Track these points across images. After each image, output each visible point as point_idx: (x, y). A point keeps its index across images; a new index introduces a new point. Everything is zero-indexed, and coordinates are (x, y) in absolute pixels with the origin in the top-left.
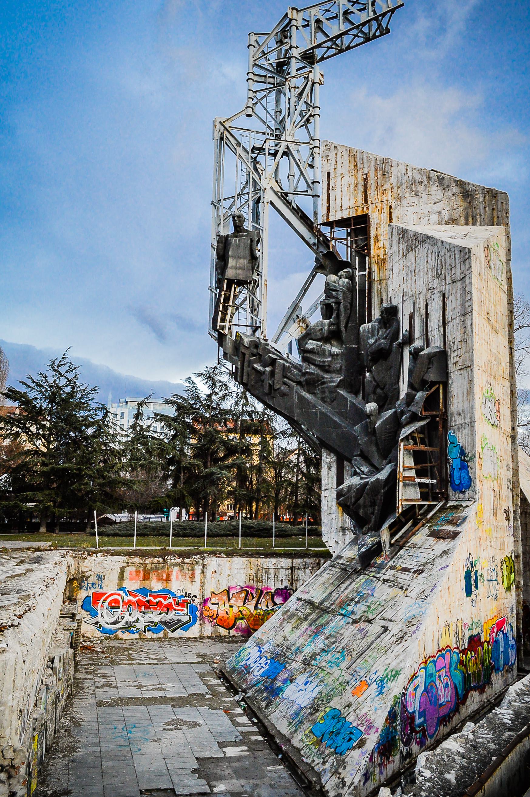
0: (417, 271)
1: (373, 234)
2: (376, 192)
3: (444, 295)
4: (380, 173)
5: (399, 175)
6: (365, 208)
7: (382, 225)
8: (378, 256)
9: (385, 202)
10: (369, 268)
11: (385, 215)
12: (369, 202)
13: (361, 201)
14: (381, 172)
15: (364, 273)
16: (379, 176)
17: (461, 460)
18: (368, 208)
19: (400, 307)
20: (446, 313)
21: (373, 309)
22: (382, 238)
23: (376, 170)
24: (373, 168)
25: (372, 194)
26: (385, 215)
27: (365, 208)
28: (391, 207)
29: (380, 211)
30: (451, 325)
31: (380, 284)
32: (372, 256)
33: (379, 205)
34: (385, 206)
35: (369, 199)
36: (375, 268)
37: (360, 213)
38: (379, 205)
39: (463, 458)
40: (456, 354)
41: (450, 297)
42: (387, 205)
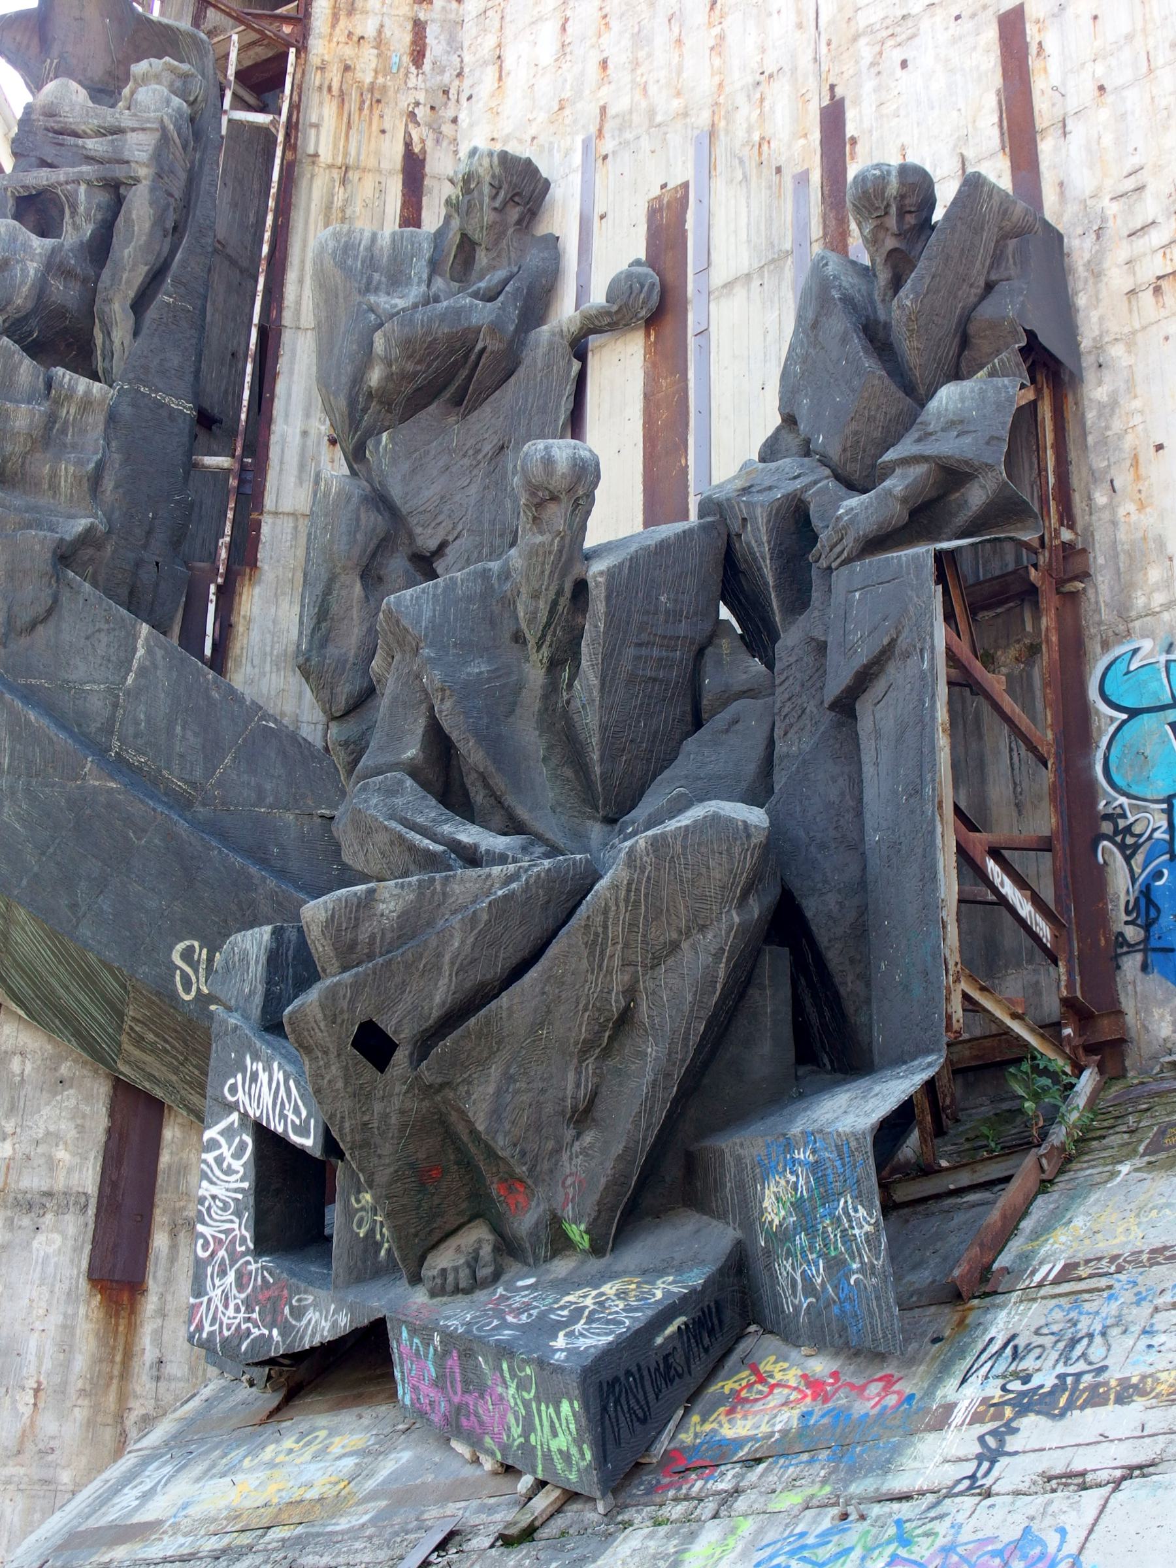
8: (347, 68)
10: (295, 107)
31: (344, 181)
32: (314, 59)
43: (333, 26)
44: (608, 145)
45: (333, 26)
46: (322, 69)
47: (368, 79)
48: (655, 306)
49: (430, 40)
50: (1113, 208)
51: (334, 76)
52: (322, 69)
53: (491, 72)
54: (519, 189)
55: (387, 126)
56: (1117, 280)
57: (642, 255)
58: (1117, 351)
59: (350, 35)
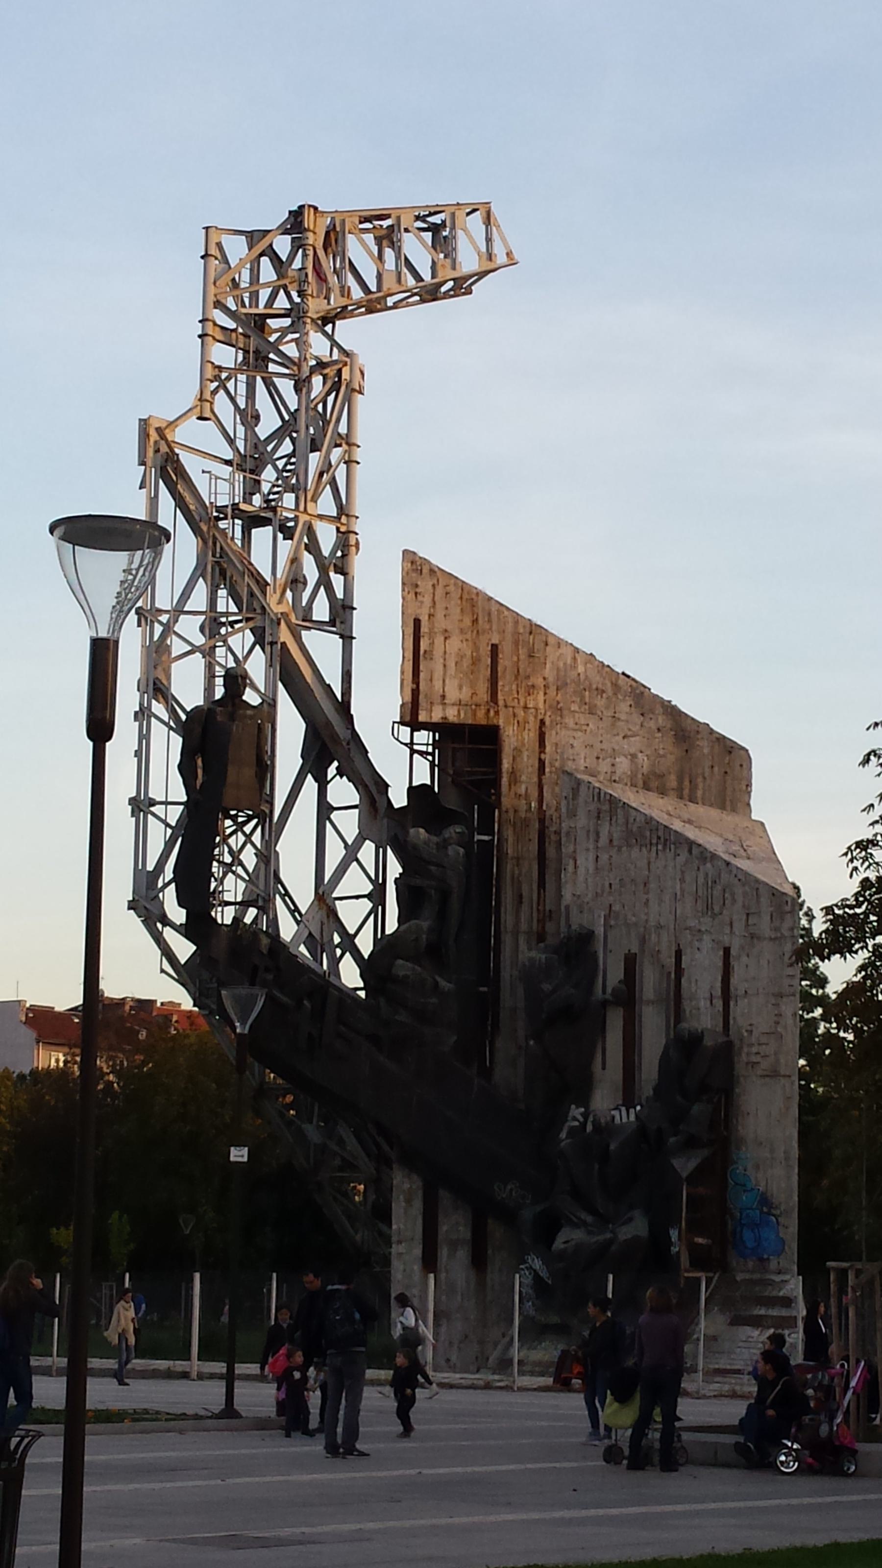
0: (652, 886)
1: (506, 765)
2: (514, 687)
3: (727, 951)
4: (523, 652)
5: (561, 665)
6: (492, 713)
7: (525, 754)
8: (516, 811)
9: (533, 710)
11: (532, 734)
12: (501, 703)
13: (483, 694)
14: (525, 650)
15: (486, 838)
16: (522, 657)
17: (762, 1212)
18: (497, 713)
19: (600, 931)
20: (734, 980)
21: (503, 910)
22: (524, 778)
23: (516, 643)
24: (509, 637)
25: (506, 689)
26: (530, 736)
27: (492, 713)
28: (542, 722)
29: (522, 725)
30: (743, 1003)
32: (504, 809)
33: (521, 713)
34: (531, 719)
35: (500, 697)
36: (509, 833)
37: (481, 718)
38: (521, 713)
39: (765, 1209)
40: (754, 1050)
41: (744, 959)
42: (536, 717)
43: (510, 790)
44: (612, 923)
45: (510, 790)
46: (507, 812)
47: (523, 816)
48: (627, 997)
49: (545, 794)
50: (745, 1034)
51: (511, 814)
52: (507, 812)
53: (571, 862)
54: (586, 937)
55: (531, 837)
56: (744, 1057)
57: (622, 977)
58: (742, 1079)
59: (516, 794)
